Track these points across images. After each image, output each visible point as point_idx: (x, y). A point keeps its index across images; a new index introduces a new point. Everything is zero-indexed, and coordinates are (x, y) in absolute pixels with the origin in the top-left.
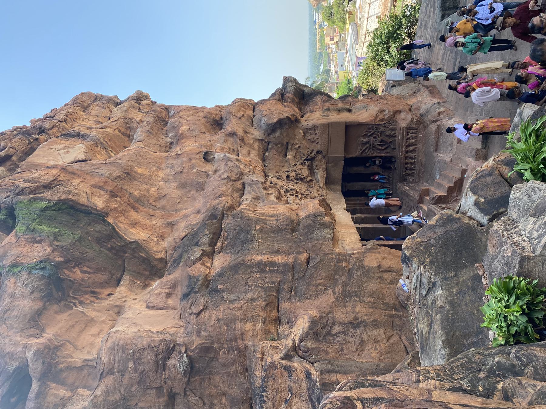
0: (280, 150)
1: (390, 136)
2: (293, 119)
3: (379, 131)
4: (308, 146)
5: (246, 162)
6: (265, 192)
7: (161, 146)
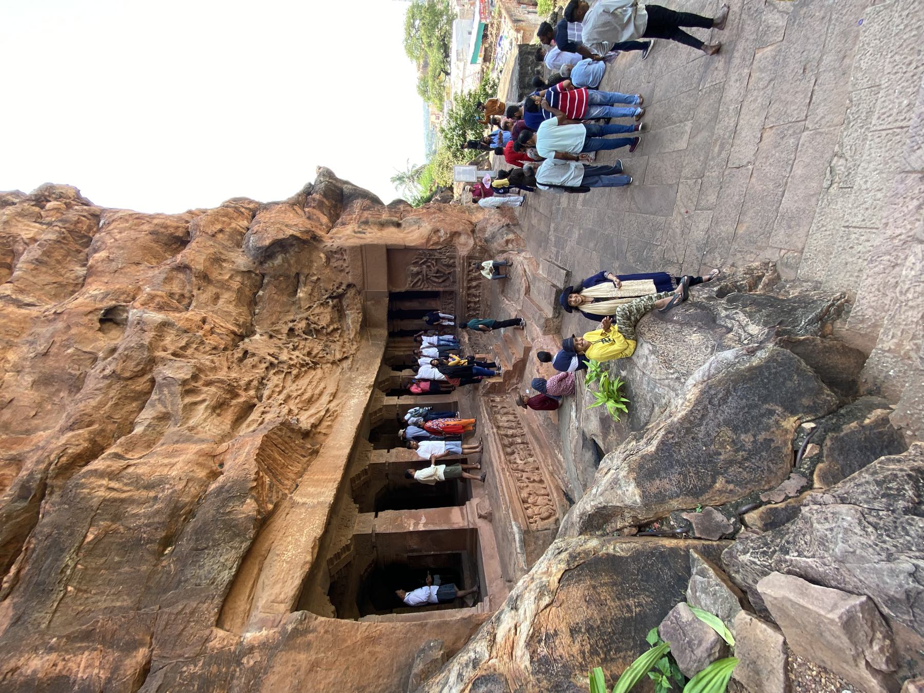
0: (283, 286)
1: (449, 266)
2: (305, 237)
3: (434, 255)
4: (333, 277)
5: (187, 325)
6: (188, 400)
7: (62, 286)
